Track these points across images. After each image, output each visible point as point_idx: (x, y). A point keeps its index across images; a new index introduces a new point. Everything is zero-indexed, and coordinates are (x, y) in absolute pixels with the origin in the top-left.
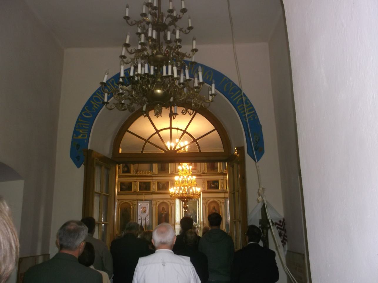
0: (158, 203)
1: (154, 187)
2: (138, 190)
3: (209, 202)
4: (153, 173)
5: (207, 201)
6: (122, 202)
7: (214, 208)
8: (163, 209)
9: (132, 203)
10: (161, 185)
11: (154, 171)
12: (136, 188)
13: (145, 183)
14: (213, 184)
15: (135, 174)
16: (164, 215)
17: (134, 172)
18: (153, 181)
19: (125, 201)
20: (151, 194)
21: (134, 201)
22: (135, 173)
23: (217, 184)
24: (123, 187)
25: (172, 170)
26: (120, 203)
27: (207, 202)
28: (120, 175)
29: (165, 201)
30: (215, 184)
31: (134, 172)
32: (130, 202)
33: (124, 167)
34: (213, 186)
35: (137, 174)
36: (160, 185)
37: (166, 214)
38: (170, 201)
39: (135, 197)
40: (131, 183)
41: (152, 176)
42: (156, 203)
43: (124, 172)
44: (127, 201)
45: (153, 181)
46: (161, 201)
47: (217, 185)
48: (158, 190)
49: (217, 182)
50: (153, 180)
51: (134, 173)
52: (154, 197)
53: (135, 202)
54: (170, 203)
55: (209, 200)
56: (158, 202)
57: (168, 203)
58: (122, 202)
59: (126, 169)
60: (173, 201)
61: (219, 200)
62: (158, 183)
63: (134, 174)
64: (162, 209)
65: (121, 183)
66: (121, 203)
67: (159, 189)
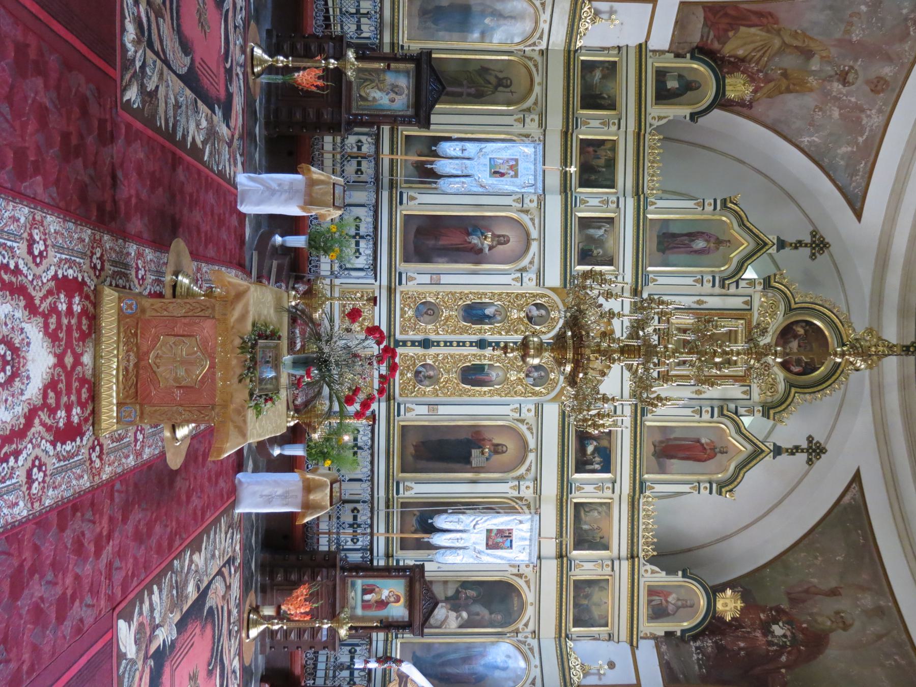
0: (525, 219)
1: (594, 202)
2: (581, 137)
3: (523, 428)
4: (651, 199)
5: (527, 423)
6: (536, 66)
7: (497, 449)
8: (502, 240)
9: (529, 110)
10: (601, 232)
11: (661, 204)
12: (593, 126)
13: (611, 164)
14: (597, 450)
15: (651, 125)
16: (475, 240)
17: (660, 118)
18: (618, 198)
19: (537, 79)
20: (565, 189)
21: (536, 118)
22: (656, 123)
23: (597, 467)
24: (598, 74)
25: (661, 280)
26: (530, 59)
27: (522, 421)
28: (650, 61)
29: (534, 247)
30: (598, 459)
31: (660, 118)
32: (536, 103)
33: (680, 77)
34: (590, 449)
35: (648, 130)
36: (599, 228)
37: (481, 251)
38: (535, 268)
39: (555, 122)
40: (612, 106)
41: (637, 194)
42: (526, 212)
43: (661, 74)
44: (537, 89)
45: (618, 198)
46: (534, 234)
47: (591, 467)
48: (580, 218)
49: (606, 468)
50: (622, 200)
51: (654, 118)
52: (554, 204)
53: (532, 127)
54: (523, 270)
55: (530, 429)
56: (532, 220)
57: (525, 262)
58: (536, 66)
59: (672, 84)
60: (534, 282)
61: (528, 470)
62: (610, 221)
63: (649, 119)
64: (499, 236)
65: (615, 62)
66: (531, 64)
67: (585, 223)
